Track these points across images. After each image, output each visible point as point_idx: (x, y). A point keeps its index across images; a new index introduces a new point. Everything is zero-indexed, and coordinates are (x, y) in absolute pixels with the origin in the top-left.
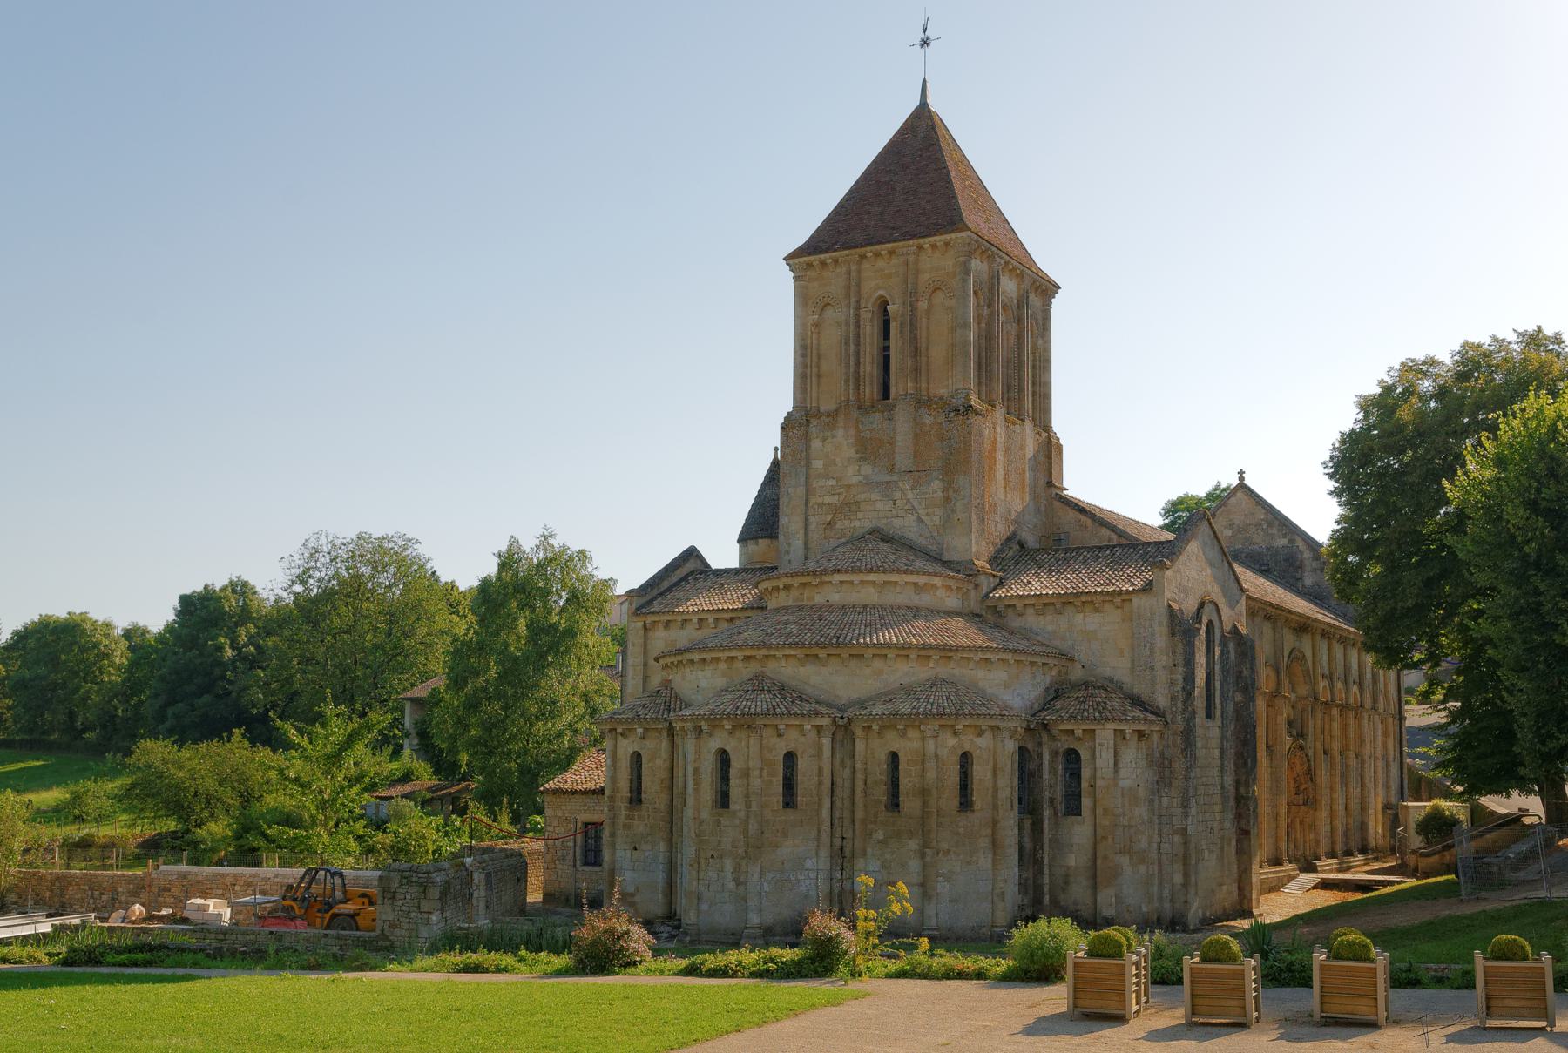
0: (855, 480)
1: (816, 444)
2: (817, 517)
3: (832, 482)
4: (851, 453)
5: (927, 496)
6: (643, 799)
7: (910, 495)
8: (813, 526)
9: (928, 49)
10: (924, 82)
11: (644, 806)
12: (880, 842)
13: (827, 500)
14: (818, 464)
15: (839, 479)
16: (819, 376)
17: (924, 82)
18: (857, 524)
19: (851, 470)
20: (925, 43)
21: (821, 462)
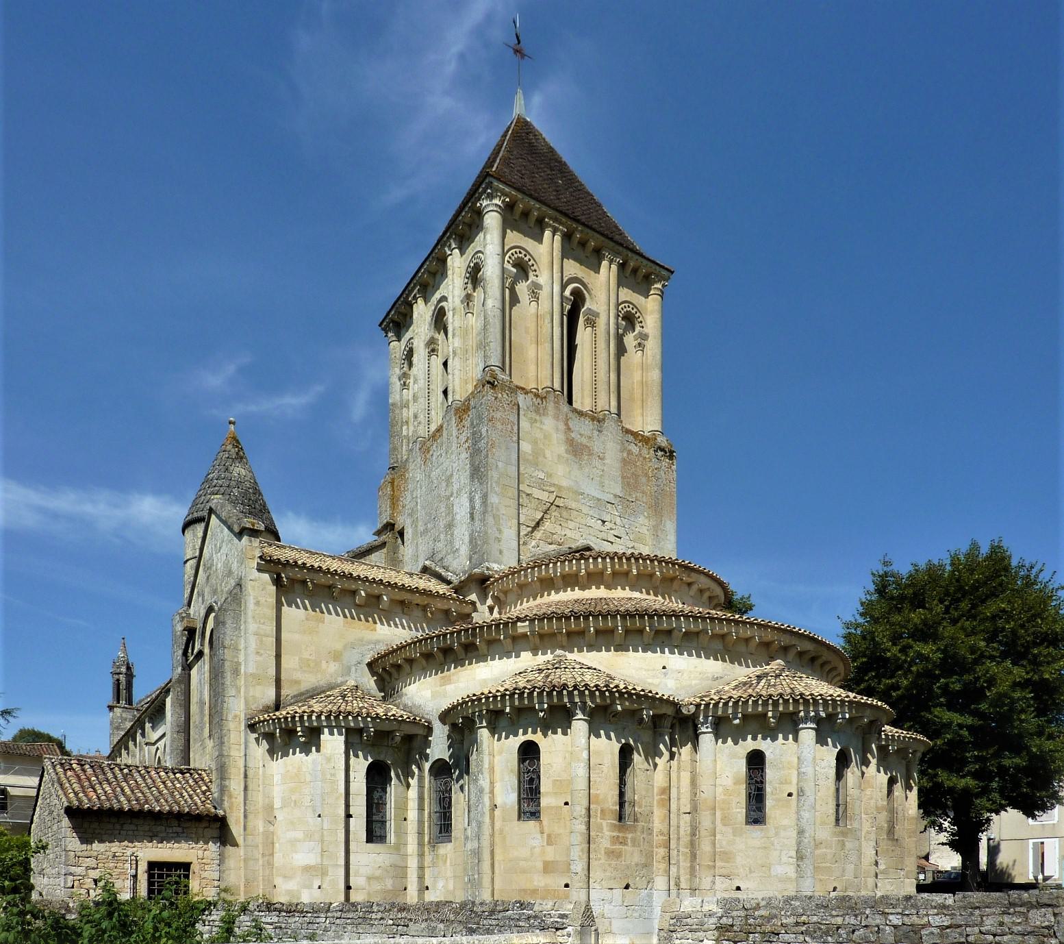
3: (542, 475)
4: (562, 449)
13: (537, 493)
18: (569, 534)
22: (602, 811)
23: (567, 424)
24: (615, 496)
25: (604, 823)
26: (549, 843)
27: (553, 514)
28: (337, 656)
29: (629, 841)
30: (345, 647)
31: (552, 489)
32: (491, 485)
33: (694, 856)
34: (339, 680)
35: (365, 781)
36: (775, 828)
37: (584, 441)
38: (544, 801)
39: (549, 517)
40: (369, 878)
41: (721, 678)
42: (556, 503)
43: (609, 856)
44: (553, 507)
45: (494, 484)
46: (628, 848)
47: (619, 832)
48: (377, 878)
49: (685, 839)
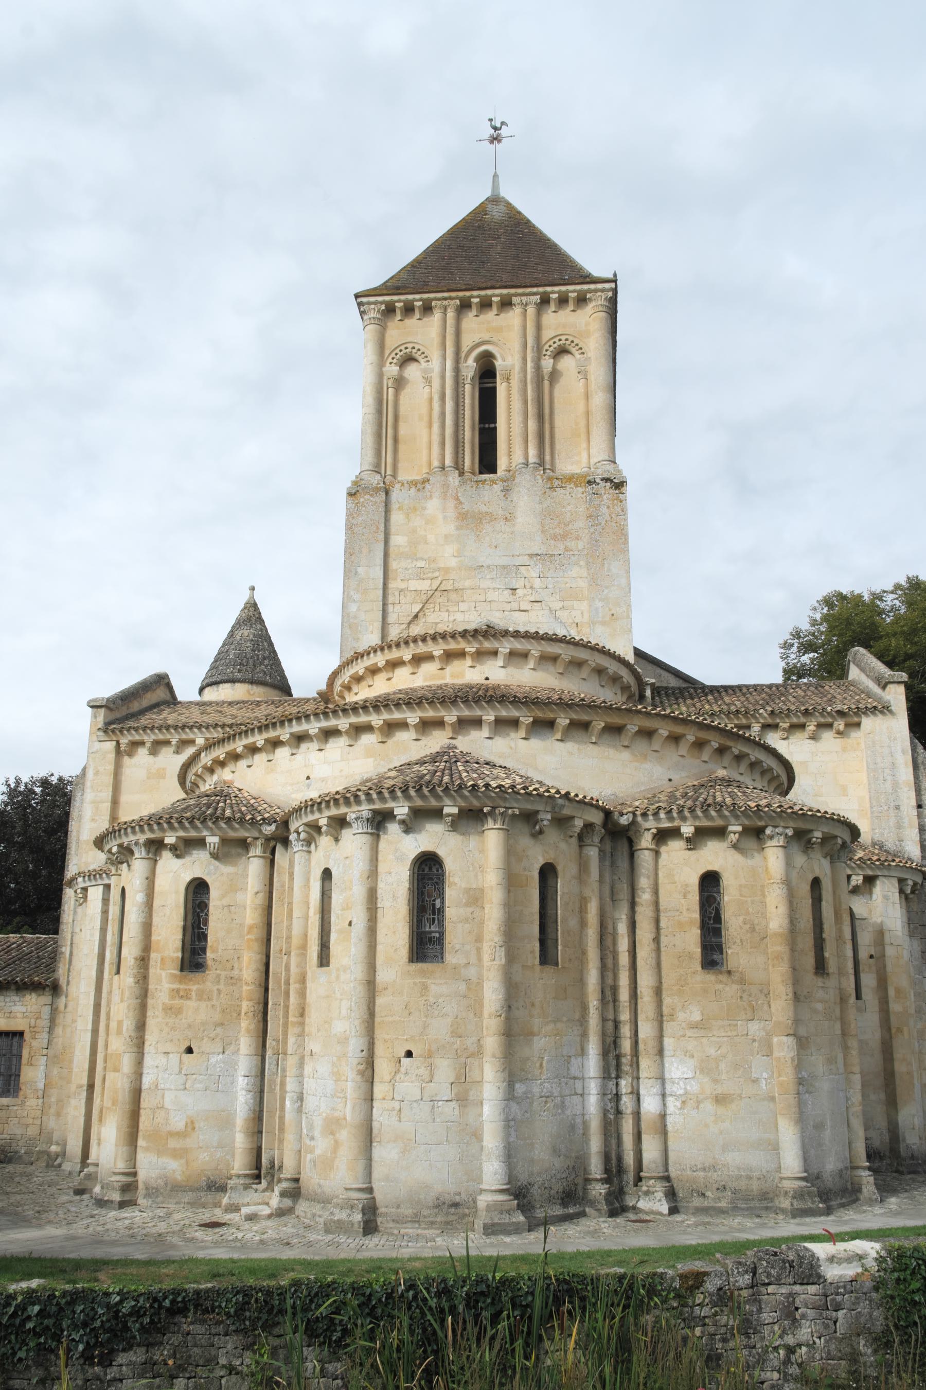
0: (453, 563)
3: (421, 564)
4: (450, 528)
7: (537, 583)
8: (392, 618)
9: (499, 147)
10: (496, 176)
13: (414, 585)
17: (496, 176)
18: (459, 617)
20: (495, 140)
21: (406, 539)
22: (162, 959)
24: (531, 556)
25: (164, 974)
29: (193, 994)
31: (436, 574)
36: (338, 970)
39: (432, 605)
42: (443, 587)
43: (166, 1013)
44: (438, 594)
46: (191, 1004)
47: (180, 982)
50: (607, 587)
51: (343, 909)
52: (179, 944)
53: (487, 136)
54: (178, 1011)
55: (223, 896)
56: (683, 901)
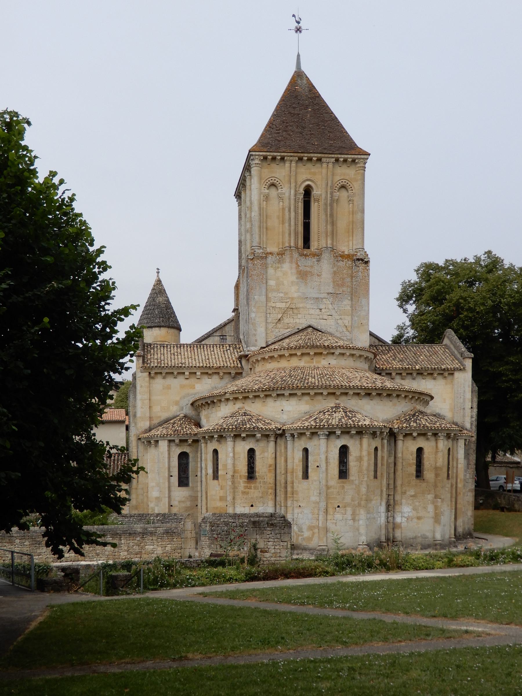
0: (295, 295)
1: (271, 271)
2: (271, 315)
3: (282, 295)
4: (293, 278)
5: (341, 308)
6: (257, 477)
9: (301, 35)
11: (258, 480)
12: (412, 496)
13: (279, 305)
14: (272, 283)
15: (286, 293)
16: (267, 228)
17: (298, 56)
18: (298, 321)
19: (294, 289)
20: (298, 30)
21: (274, 282)
23: (297, 264)
24: (328, 293)
25: (241, 481)
26: (221, 489)
27: (289, 313)
28: (177, 403)
30: (180, 398)
31: (287, 300)
32: (251, 309)
33: (286, 492)
34: (178, 413)
35: (177, 461)
37: (308, 269)
38: (220, 473)
39: (286, 315)
40: (179, 502)
41: (308, 412)
45: (253, 308)
46: (252, 491)
47: (248, 484)
48: (183, 502)
49: (283, 485)
50: (360, 311)
51: (314, 462)
52: (247, 471)
53: (293, 27)
54: (247, 493)
55: (261, 454)
56: (411, 457)
